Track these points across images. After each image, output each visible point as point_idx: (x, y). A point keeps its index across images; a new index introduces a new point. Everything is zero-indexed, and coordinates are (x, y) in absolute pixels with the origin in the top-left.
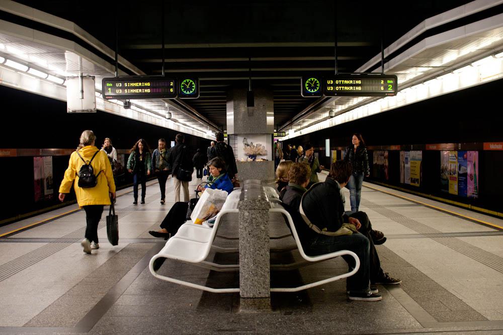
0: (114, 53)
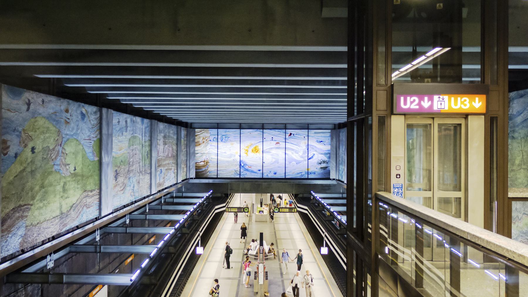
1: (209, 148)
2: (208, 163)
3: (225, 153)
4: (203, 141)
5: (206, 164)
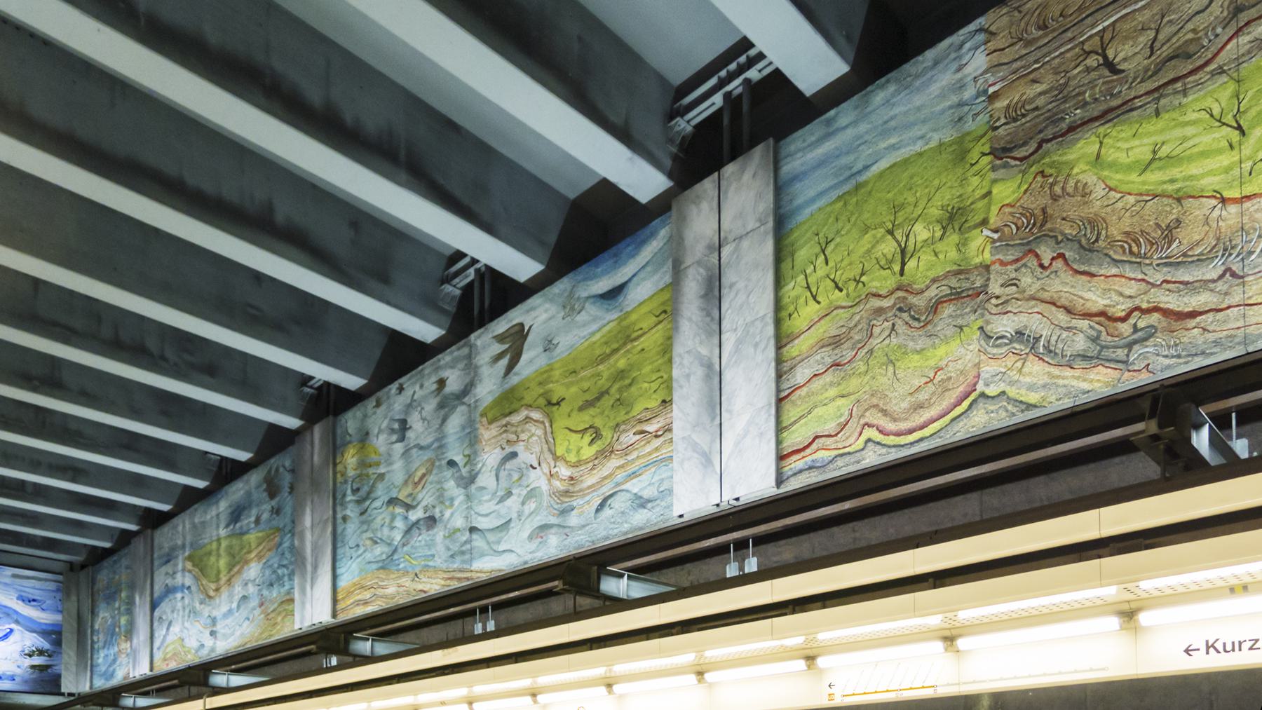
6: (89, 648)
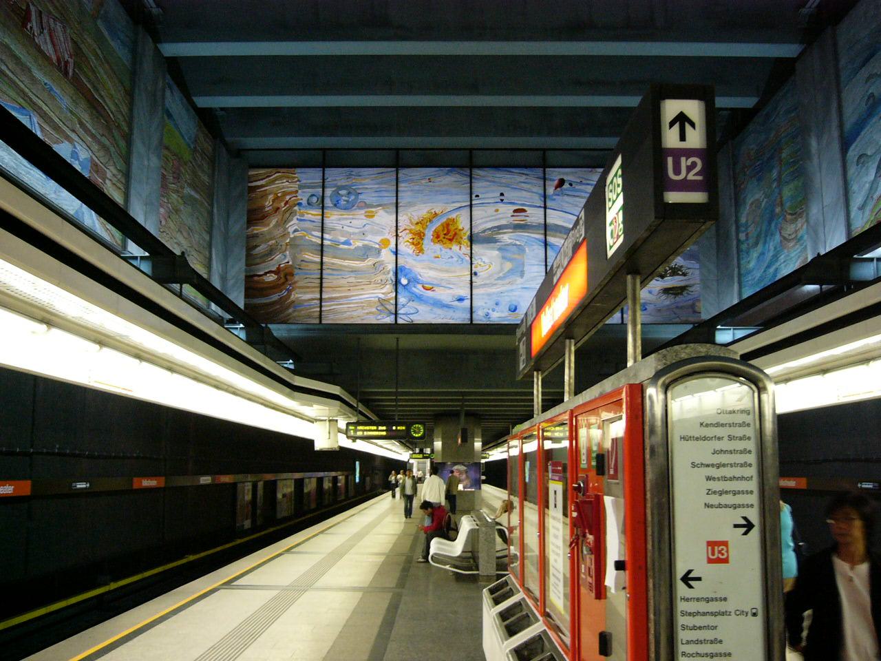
0: (356, 401)
1: (296, 227)
2: (289, 277)
3: (347, 243)
4: (276, 205)
5: (283, 280)
6: (735, 252)
